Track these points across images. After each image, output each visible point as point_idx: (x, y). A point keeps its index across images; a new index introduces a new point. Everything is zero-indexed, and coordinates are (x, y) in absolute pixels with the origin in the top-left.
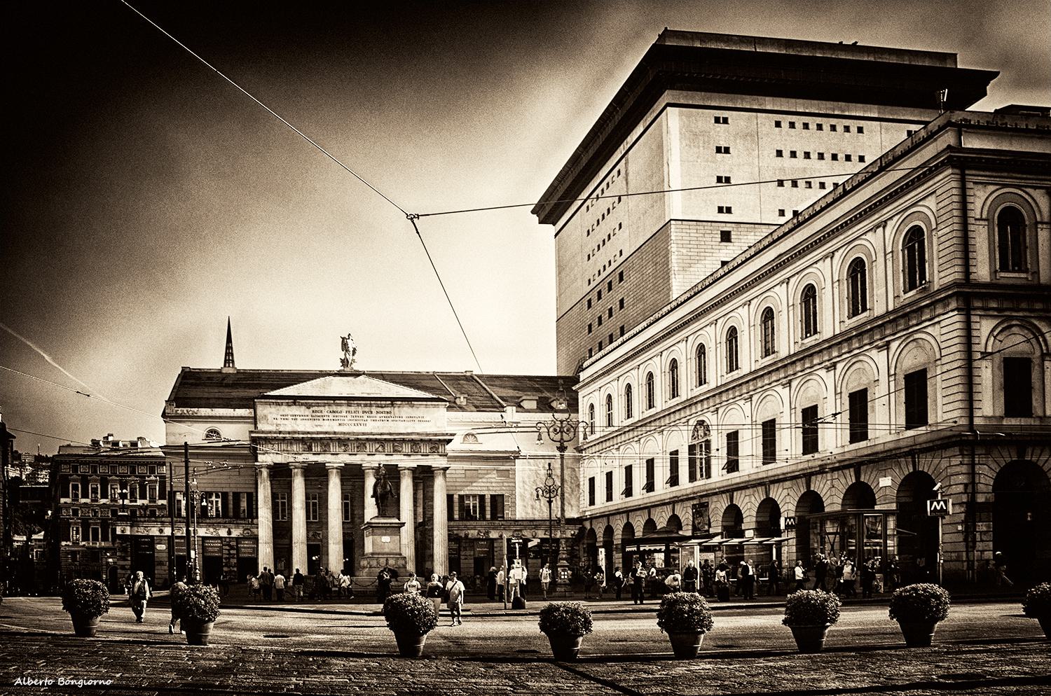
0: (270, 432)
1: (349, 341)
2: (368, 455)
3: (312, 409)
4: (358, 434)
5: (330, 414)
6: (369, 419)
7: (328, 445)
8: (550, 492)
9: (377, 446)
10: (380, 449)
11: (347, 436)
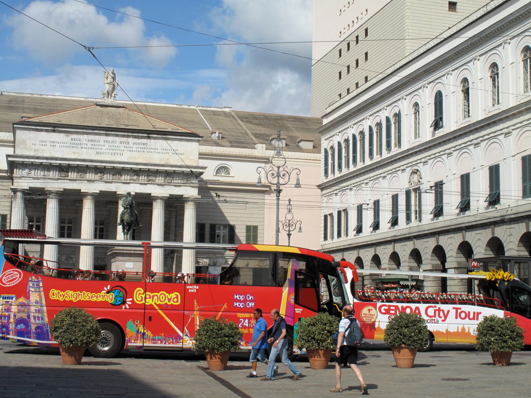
0: (28, 157)
2: (124, 183)
5: (88, 143)
6: (126, 149)
8: (289, 226)
11: (104, 164)
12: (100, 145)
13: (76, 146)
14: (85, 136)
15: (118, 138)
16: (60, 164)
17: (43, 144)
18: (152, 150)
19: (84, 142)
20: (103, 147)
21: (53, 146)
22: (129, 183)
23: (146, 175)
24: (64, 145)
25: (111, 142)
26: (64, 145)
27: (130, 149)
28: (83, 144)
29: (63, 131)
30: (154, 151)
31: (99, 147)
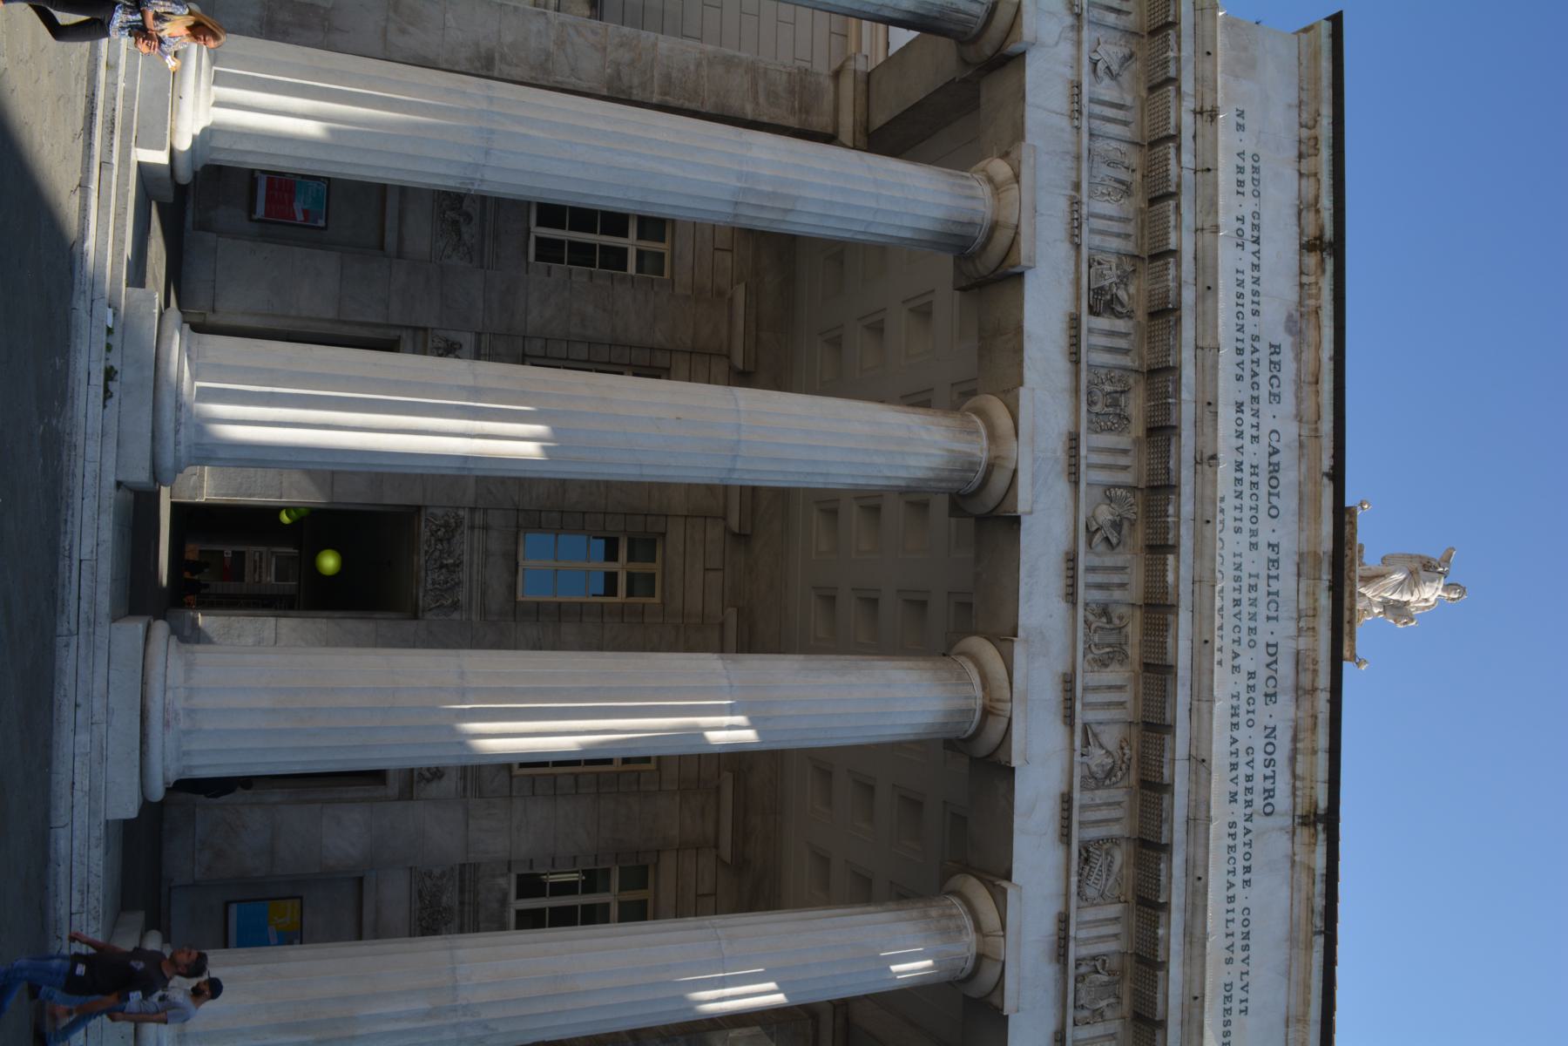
1: (1430, 593)
2: (1068, 682)
3: (1286, 341)
4: (1203, 614)
5: (1263, 447)
9: (1110, 737)
10: (1098, 758)
12: (1254, 520)
13: (1247, 374)
14: (1290, 430)
15: (1291, 628)
16: (1174, 253)
17: (1247, 176)
18: (1241, 850)
19: (1267, 424)
20: (1245, 538)
21: (1240, 233)
22: (1069, 718)
23: (1116, 830)
25: (1275, 585)
27: (1242, 711)
28: (1256, 414)
29: (1318, 297)
30: (1240, 864)
31: (1247, 514)
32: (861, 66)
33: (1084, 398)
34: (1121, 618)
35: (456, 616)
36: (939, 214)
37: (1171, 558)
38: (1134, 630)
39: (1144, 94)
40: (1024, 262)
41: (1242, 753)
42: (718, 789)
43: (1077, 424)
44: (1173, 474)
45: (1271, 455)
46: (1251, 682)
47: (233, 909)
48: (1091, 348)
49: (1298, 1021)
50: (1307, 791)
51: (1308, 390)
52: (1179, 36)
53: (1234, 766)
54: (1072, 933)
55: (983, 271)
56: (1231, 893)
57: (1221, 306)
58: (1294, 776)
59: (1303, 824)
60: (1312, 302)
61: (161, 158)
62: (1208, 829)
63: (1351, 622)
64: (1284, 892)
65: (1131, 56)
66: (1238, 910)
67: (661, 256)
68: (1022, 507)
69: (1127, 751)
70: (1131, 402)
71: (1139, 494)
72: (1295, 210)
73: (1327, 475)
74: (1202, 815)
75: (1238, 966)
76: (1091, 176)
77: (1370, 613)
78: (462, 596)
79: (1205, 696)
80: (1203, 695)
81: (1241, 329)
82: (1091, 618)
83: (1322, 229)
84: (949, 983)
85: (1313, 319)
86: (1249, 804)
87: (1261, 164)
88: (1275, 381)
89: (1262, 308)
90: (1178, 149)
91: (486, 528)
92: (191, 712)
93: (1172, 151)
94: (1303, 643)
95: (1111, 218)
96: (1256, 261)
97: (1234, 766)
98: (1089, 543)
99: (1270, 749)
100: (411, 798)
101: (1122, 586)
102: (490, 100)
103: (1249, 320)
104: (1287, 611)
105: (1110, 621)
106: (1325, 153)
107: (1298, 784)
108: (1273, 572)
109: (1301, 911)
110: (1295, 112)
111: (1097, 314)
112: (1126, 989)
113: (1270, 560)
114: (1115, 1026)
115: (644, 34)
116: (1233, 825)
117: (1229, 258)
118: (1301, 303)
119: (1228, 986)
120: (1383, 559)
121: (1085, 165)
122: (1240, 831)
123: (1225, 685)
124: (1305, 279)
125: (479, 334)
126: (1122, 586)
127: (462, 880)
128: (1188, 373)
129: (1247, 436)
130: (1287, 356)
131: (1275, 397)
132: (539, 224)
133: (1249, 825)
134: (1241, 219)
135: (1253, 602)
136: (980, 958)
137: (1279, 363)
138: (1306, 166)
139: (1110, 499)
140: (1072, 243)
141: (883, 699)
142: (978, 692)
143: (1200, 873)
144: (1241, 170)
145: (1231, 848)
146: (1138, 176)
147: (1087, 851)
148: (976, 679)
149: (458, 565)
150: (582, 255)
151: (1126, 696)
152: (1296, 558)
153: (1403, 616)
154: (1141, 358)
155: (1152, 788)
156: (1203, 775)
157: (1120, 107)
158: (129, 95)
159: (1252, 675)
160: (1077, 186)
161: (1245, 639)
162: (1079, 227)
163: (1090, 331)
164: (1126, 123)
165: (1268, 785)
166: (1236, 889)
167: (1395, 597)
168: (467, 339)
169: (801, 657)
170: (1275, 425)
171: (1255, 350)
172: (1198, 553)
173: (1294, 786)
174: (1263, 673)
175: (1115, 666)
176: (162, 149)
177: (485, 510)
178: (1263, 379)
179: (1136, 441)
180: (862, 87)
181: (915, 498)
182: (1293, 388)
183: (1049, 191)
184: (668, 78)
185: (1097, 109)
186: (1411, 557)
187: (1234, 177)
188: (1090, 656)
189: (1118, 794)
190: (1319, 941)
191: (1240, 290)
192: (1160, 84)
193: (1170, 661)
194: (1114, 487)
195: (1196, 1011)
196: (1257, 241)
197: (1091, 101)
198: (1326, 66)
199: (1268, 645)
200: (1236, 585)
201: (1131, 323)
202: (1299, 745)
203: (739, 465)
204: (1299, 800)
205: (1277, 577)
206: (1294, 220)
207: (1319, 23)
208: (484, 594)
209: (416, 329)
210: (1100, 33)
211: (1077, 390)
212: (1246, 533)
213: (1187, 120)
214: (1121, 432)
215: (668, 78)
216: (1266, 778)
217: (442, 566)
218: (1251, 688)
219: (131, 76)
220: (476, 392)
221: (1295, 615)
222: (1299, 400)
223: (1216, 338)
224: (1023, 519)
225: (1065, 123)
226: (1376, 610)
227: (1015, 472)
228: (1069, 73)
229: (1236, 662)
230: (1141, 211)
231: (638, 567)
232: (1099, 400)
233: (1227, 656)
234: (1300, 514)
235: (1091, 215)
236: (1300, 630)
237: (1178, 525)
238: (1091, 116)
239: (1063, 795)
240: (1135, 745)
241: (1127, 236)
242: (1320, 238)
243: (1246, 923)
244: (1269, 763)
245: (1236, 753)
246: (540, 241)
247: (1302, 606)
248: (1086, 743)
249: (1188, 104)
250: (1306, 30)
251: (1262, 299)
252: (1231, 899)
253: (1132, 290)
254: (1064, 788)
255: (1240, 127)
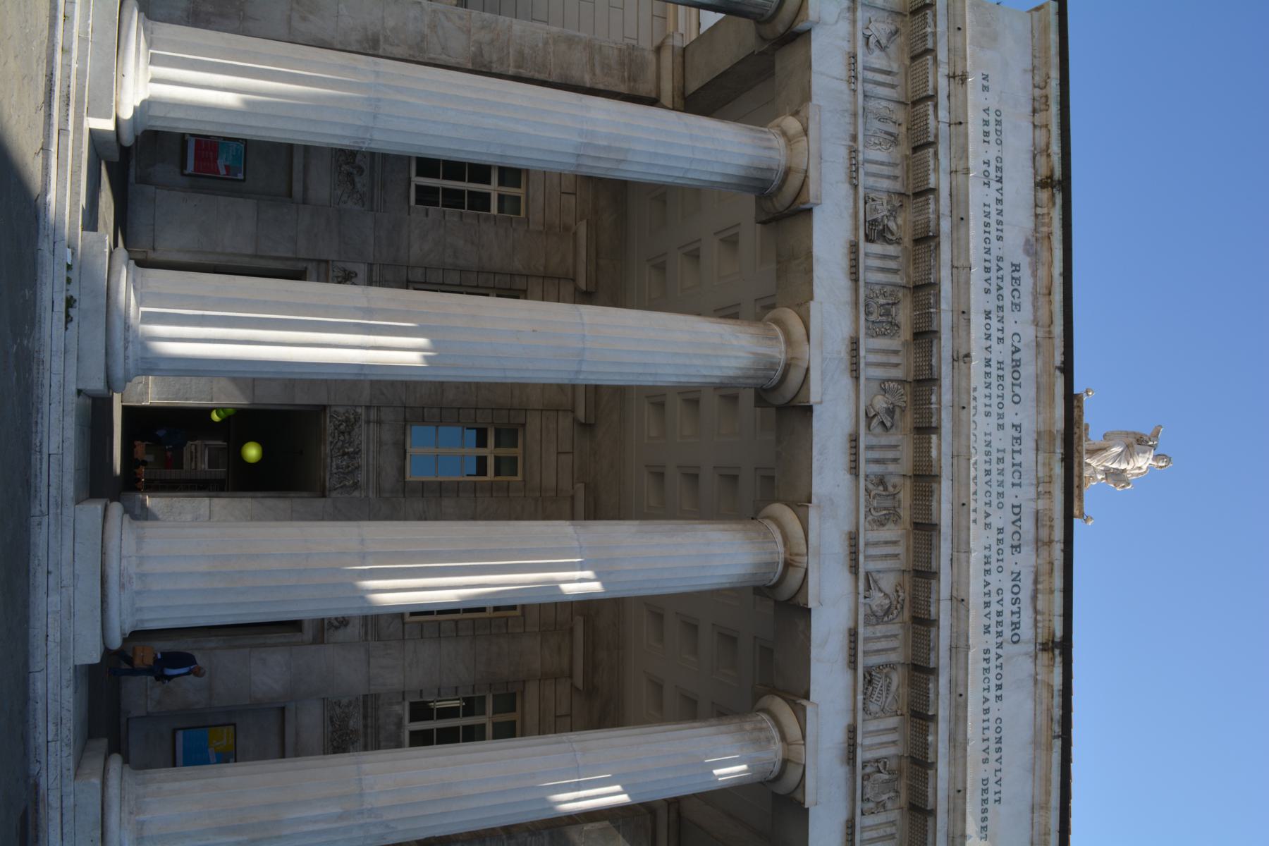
1: (1143, 462)
2: (853, 538)
3: (1024, 261)
4: (961, 482)
5: (1007, 347)
6: (993, 533)
7: (884, 324)
9: (888, 583)
10: (878, 600)
12: (1001, 405)
13: (993, 288)
14: (1029, 333)
15: (1033, 494)
16: (933, 191)
17: (991, 128)
18: (994, 672)
19: (1010, 328)
20: (993, 420)
21: (986, 174)
22: (854, 568)
23: (893, 657)
24: (993, 221)
26: (993, 221)
27: (993, 560)
28: (1001, 320)
29: (1049, 225)
30: (993, 682)
31: (995, 401)
32: (678, 43)
33: (862, 309)
34: (895, 487)
35: (356, 494)
36: (743, 162)
37: (934, 437)
38: (905, 497)
39: (907, 62)
40: (812, 200)
41: (994, 594)
42: (572, 630)
43: (857, 330)
44: (935, 369)
45: (1013, 353)
46: (1000, 536)
47: (180, 735)
48: (867, 268)
49: (1042, 808)
50: (1047, 623)
51: (1042, 301)
52: (935, 16)
53: (987, 604)
54: (859, 740)
55: (779, 207)
56: (986, 706)
57: (972, 233)
58: (1036, 611)
59: (1044, 650)
60: (1045, 229)
61: (108, 125)
62: (967, 655)
63: (1080, 487)
64: (1029, 705)
65: (896, 32)
66: (992, 720)
67: (519, 198)
68: (814, 398)
69: (901, 593)
70: (901, 312)
71: (907, 387)
72: (1029, 156)
73: (1059, 368)
74: (962, 644)
75: (993, 765)
76: (865, 129)
77: (1095, 479)
78: (361, 477)
79: (963, 547)
80: (961, 547)
81: (988, 251)
82: (871, 487)
83: (1052, 171)
84: (761, 783)
85: (1046, 242)
86: (1000, 634)
87: (1003, 118)
88: (1016, 293)
89: (1004, 235)
90: (936, 106)
91: (379, 422)
92: (142, 576)
93: (931, 109)
94: (1041, 504)
95: (882, 163)
96: (999, 197)
97: (987, 604)
98: (868, 427)
99: (1016, 590)
100: (323, 642)
101: (895, 460)
102: (377, 74)
103: (995, 244)
104: (1028, 478)
105: (886, 489)
106: (1054, 108)
107: (1039, 618)
108: (1017, 448)
109: (1042, 719)
110: (1029, 76)
111: (872, 241)
112: (903, 785)
113: (1014, 438)
114: (894, 815)
115: (501, 18)
116: (987, 651)
117: (977, 195)
118: (1036, 230)
119: (985, 781)
120: (1105, 436)
121: (860, 121)
122: (992, 656)
123: (979, 539)
124: (1039, 211)
125: (371, 265)
126: (895, 460)
127: (365, 707)
128: (946, 288)
129: (994, 339)
130: (1025, 273)
131: (1016, 306)
132: (418, 174)
133: (1000, 651)
134: (987, 163)
135: (1001, 472)
136: (785, 762)
137: (1019, 279)
138: (1039, 119)
139: (885, 391)
140: (851, 183)
141: (704, 555)
142: (781, 548)
143: (961, 690)
144: (986, 123)
145: (986, 670)
146: (903, 129)
147: (870, 675)
148: (779, 538)
149: (357, 452)
150: (453, 199)
151: (899, 549)
152: (1035, 436)
153: (1121, 481)
154: (908, 276)
155: (923, 624)
156: (963, 612)
157: (888, 73)
158: (81, 74)
159: (1000, 531)
160: (854, 138)
161: (995, 503)
162: (857, 171)
163: (866, 254)
164: (893, 86)
165: (1015, 619)
166: (990, 702)
167: (1115, 466)
168: (361, 269)
169: (637, 522)
170: (1016, 329)
171: (1000, 269)
172: (956, 433)
173: (1036, 621)
174: (1010, 529)
175: (890, 526)
176: (109, 117)
177: (379, 408)
178: (1007, 292)
179: (905, 344)
180: (679, 59)
181: (727, 392)
182: (1030, 298)
183: (831, 141)
184: (521, 53)
185: (870, 75)
186: (1127, 434)
187: (981, 128)
188: (870, 518)
189: (894, 628)
190: (1058, 743)
191: (987, 220)
192: (921, 54)
193: (935, 520)
194: (888, 381)
195: (960, 801)
196: (1000, 180)
197: (865, 68)
198: (1054, 37)
199: (1013, 506)
200: (987, 458)
201: (899, 248)
202: (1040, 586)
203: (584, 368)
204: (1039, 631)
205: (1020, 452)
206: (1030, 163)
207: (1048, 3)
208: (379, 475)
209: (319, 261)
210: (871, 14)
211: (856, 303)
212: (994, 416)
213: (943, 83)
214: (892, 336)
215: (521, 53)
216: (1013, 613)
217: (344, 454)
218: (1000, 541)
219: (82, 58)
220: (369, 312)
221: (1034, 482)
222: (1035, 309)
223: (968, 260)
224: (815, 408)
225: (844, 87)
226: (1100, 477)
227: (808, 370)
228: (846, 46)
229: (988, 520)
230: (906, 156)
231: (504, 452)
232: (875, 311)
233: (980, 516)
234: (1038, 401)
235: (866, 161)
236: (1038, 494)
237: (939, 410)
238: (865, 81)
239: (850, 630)
240: (907, 588)
241: (896, 178)
242: (1051, 177)
243: (998, 730)
244: (1016, 601)
245: (989, 594)
246: (419, 188)
247: (1040, 474)
248: (868, 588)
249: (943, 70)
250: (1037, 9)
251: (1004, 227)
252: (986, 711)
253: (900, 221)
254: (851, 625)
255: (985, 88)
